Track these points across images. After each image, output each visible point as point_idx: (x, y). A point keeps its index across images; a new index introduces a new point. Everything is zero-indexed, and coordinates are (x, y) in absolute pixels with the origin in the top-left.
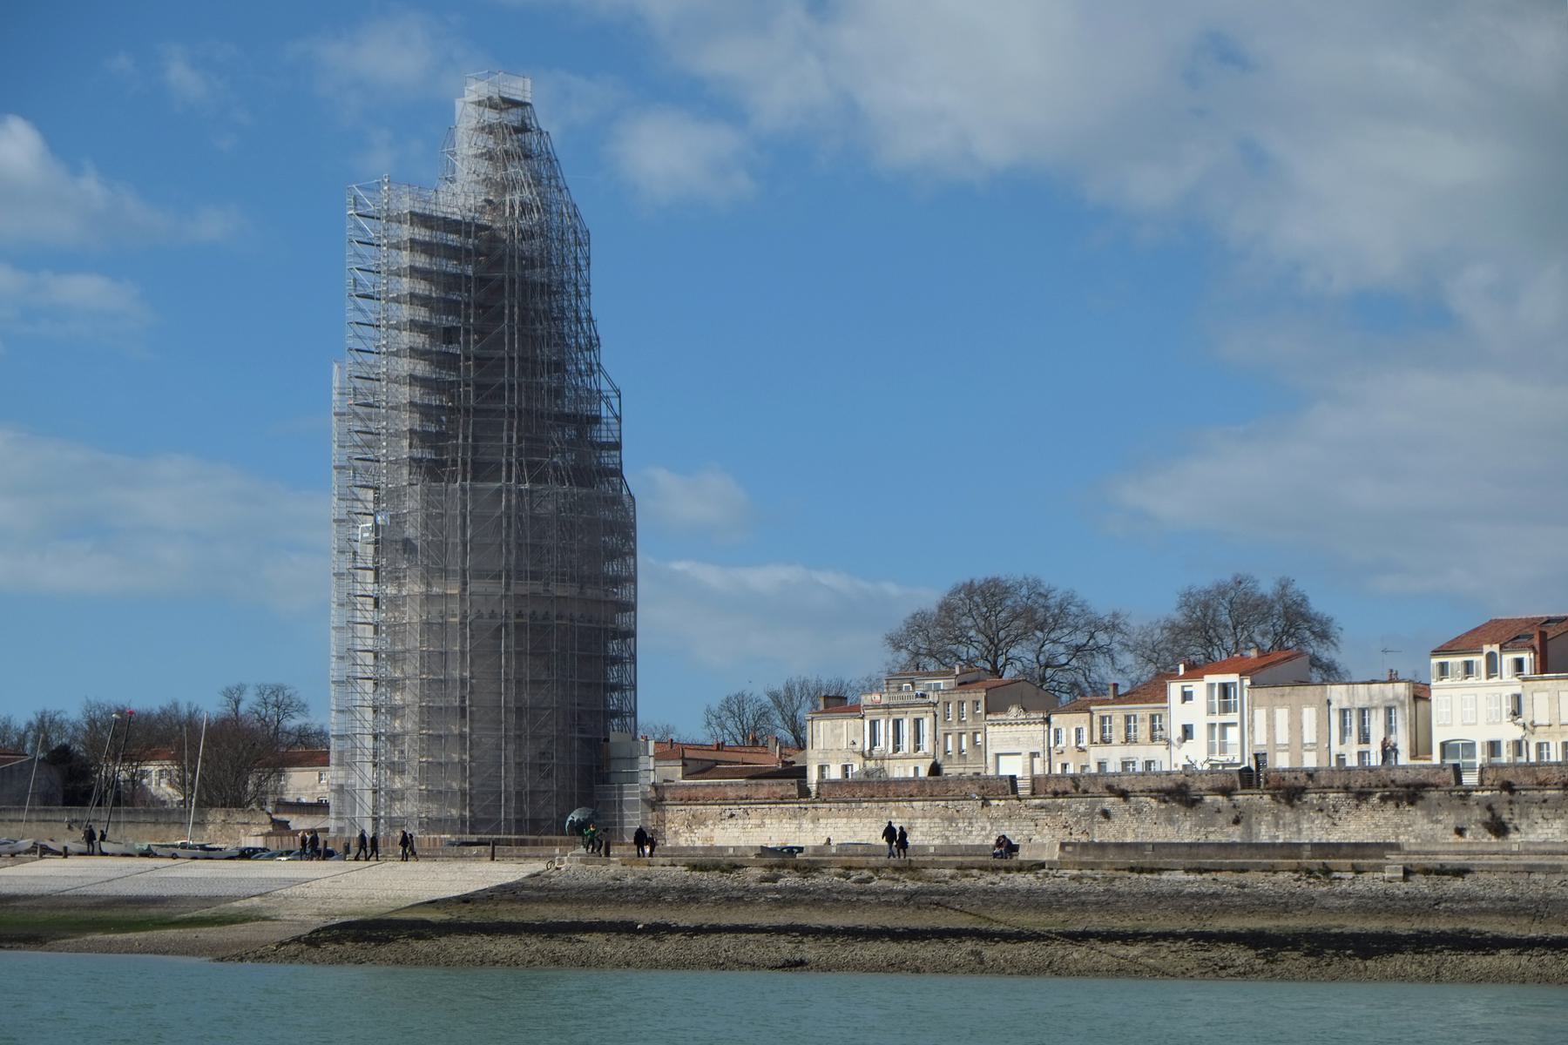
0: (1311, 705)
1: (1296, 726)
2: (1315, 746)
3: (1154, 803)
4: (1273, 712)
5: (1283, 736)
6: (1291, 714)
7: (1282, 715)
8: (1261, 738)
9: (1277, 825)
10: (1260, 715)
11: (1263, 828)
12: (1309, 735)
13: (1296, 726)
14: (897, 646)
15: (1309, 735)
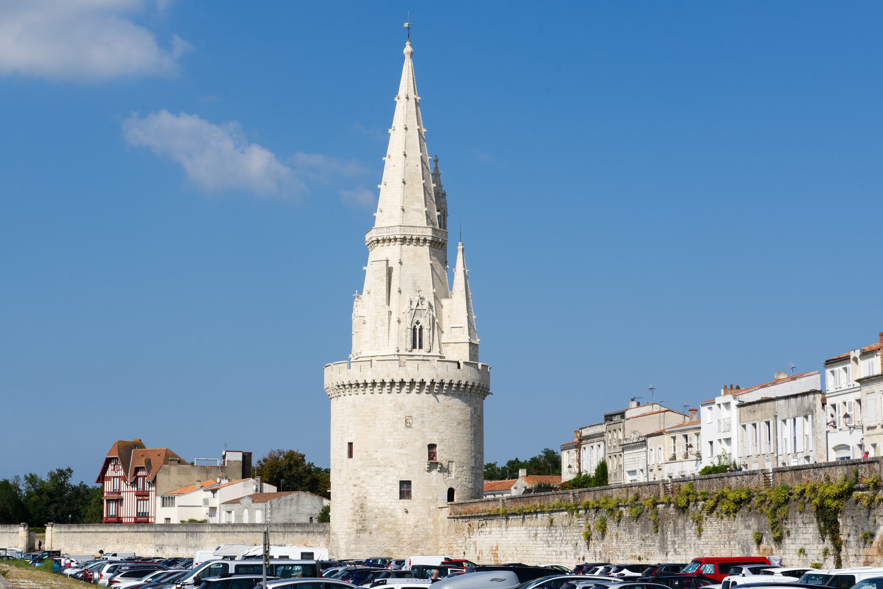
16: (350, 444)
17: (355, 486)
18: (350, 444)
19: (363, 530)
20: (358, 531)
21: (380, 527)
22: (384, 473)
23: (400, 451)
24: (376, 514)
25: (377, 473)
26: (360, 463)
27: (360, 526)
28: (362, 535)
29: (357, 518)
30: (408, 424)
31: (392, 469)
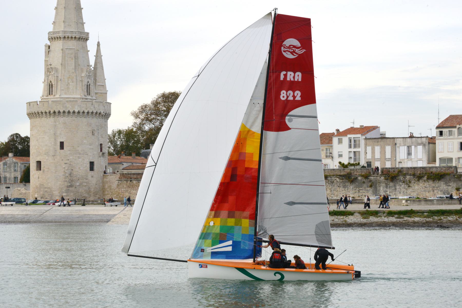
0: (389, 145)
1: (383, 152)
2: (389, 160)
3: (338, 180)
4: (374, 148)
5: (377, 155)
6: (381, 148)
7: (377, 149)
8: (369, 156)
9: (387, 187)
10: (369, 149)
11: (381, 188)
12: (388, 155)
13: (383, 152)
14: (137, 116)
15: (388, 155)
16: (101, 145)
17: (65, 163)
18: (101, 145)
19: (71, 186)
20: (68, 187)
21: (81, 184)
22: (82, 158)
23: (90, 147)
24: (79, 178)
25: (79, 158)
26: (69, 152)
27: (69, 184)
28: (70, 189)
29: (67, 180)
30: (93, 134)
31: (87, 156)
